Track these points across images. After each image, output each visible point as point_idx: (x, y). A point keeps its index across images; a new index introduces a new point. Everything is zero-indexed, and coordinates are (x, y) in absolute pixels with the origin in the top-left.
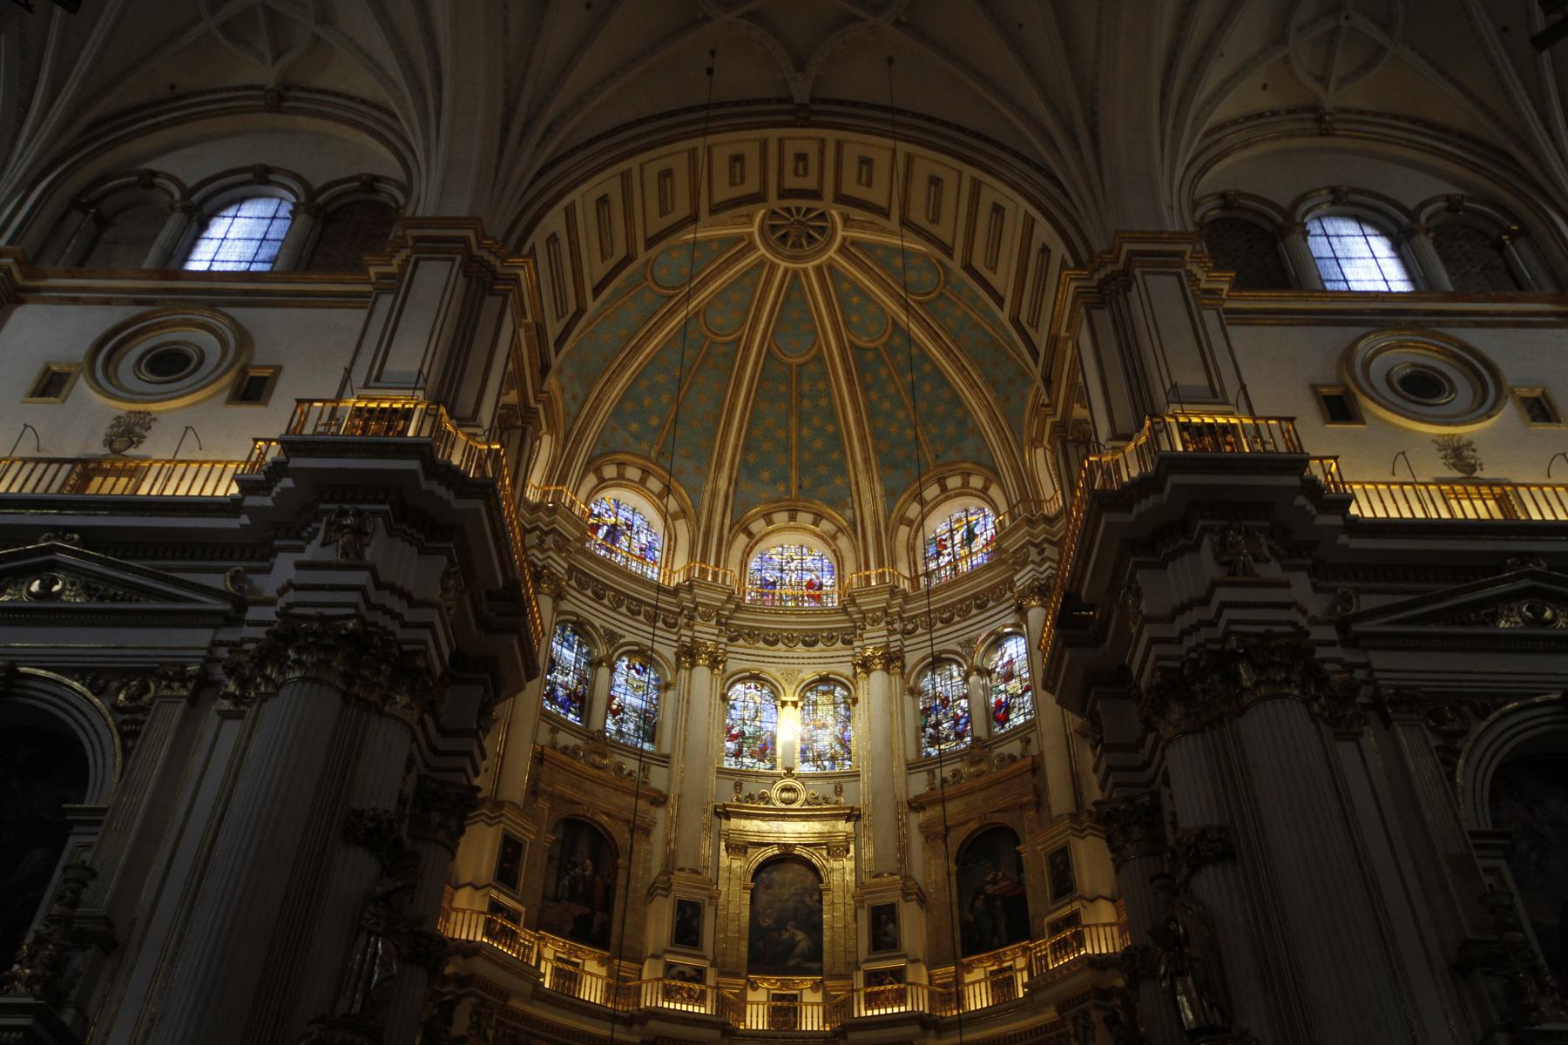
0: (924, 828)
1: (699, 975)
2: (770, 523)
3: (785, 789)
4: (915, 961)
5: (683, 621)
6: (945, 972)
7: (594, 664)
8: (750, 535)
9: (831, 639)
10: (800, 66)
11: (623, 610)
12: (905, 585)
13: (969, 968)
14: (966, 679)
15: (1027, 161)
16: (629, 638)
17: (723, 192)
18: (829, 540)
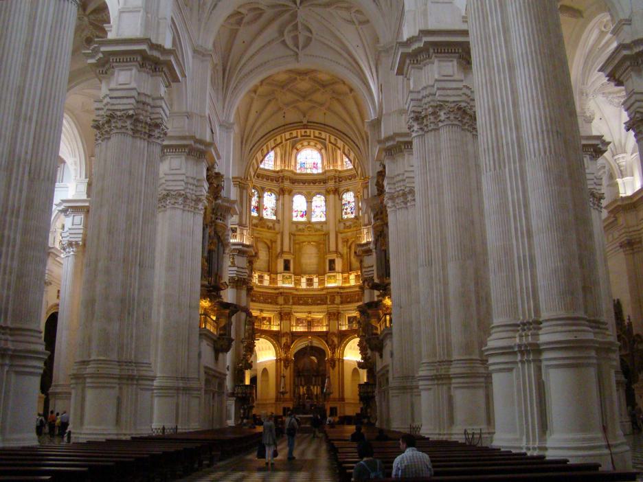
0: (343, 239)
1: (290, 277)
2: (303, 146)
3: (309, 227)
4: (339, 273)
5: (280, 180)
6: (346, 275)
7: (259, 197)
8: (297, 150)
9: (320, 182)
10: (305, 116)
11: (265, 180)
12: (339, 168)
13: (351, 274)
14: (354, 197)
15: (354, 143)
16: (267, 188)
17: (288, 137)
18: (320, 150)
